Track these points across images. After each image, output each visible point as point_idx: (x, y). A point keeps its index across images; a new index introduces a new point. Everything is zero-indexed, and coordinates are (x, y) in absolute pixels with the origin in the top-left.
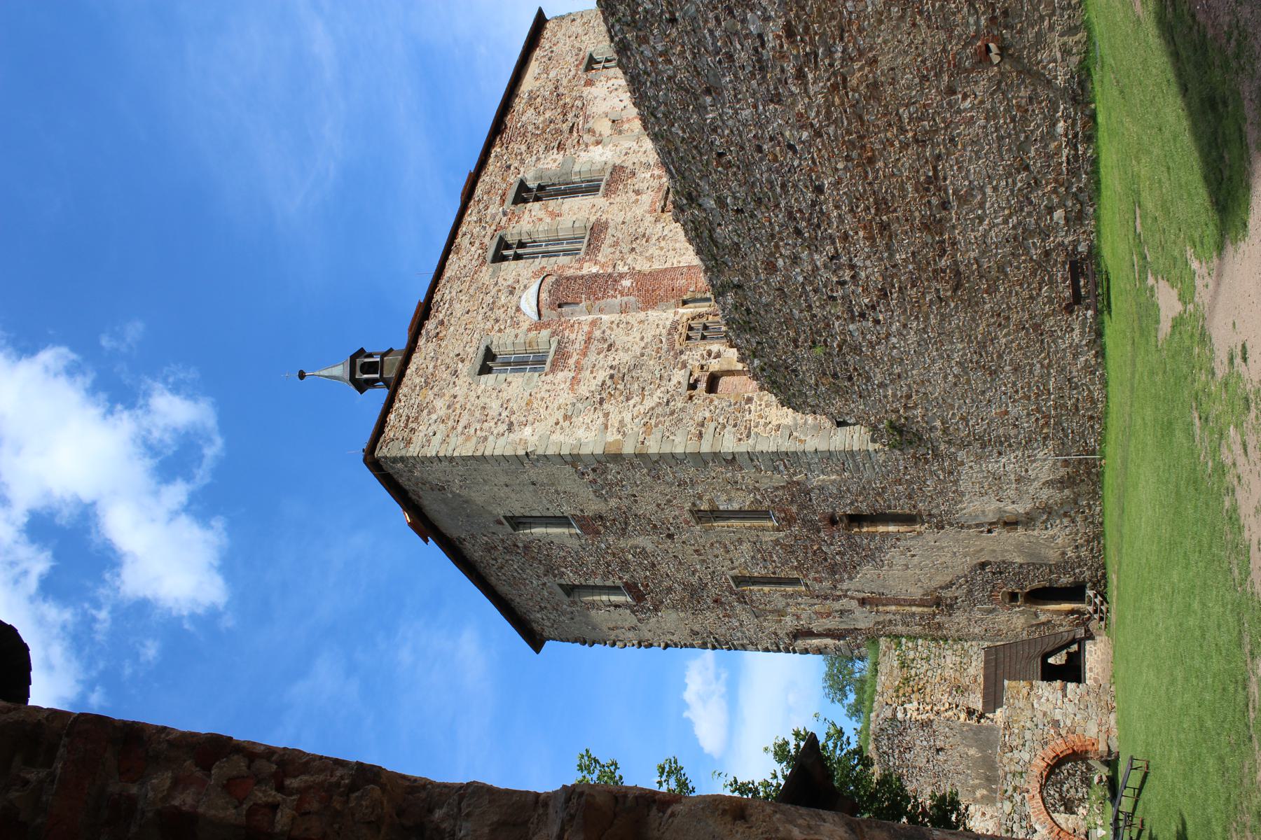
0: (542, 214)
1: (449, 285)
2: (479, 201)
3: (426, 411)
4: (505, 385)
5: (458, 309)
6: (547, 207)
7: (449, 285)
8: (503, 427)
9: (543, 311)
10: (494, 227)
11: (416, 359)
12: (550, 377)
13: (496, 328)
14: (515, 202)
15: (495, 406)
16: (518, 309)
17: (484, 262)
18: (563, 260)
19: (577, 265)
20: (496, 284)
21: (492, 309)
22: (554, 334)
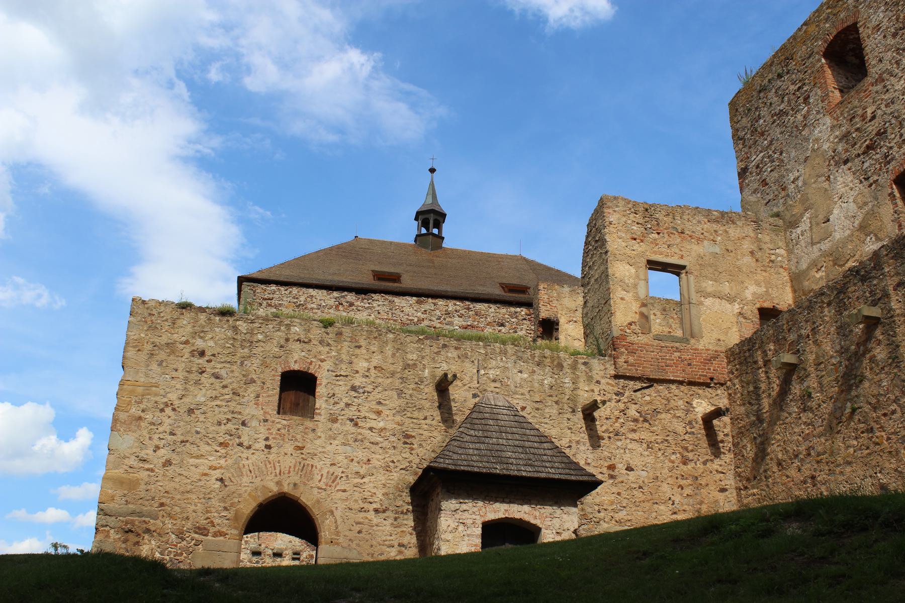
1: (386, 303)
2: (468, 309)
7: (386, 303)
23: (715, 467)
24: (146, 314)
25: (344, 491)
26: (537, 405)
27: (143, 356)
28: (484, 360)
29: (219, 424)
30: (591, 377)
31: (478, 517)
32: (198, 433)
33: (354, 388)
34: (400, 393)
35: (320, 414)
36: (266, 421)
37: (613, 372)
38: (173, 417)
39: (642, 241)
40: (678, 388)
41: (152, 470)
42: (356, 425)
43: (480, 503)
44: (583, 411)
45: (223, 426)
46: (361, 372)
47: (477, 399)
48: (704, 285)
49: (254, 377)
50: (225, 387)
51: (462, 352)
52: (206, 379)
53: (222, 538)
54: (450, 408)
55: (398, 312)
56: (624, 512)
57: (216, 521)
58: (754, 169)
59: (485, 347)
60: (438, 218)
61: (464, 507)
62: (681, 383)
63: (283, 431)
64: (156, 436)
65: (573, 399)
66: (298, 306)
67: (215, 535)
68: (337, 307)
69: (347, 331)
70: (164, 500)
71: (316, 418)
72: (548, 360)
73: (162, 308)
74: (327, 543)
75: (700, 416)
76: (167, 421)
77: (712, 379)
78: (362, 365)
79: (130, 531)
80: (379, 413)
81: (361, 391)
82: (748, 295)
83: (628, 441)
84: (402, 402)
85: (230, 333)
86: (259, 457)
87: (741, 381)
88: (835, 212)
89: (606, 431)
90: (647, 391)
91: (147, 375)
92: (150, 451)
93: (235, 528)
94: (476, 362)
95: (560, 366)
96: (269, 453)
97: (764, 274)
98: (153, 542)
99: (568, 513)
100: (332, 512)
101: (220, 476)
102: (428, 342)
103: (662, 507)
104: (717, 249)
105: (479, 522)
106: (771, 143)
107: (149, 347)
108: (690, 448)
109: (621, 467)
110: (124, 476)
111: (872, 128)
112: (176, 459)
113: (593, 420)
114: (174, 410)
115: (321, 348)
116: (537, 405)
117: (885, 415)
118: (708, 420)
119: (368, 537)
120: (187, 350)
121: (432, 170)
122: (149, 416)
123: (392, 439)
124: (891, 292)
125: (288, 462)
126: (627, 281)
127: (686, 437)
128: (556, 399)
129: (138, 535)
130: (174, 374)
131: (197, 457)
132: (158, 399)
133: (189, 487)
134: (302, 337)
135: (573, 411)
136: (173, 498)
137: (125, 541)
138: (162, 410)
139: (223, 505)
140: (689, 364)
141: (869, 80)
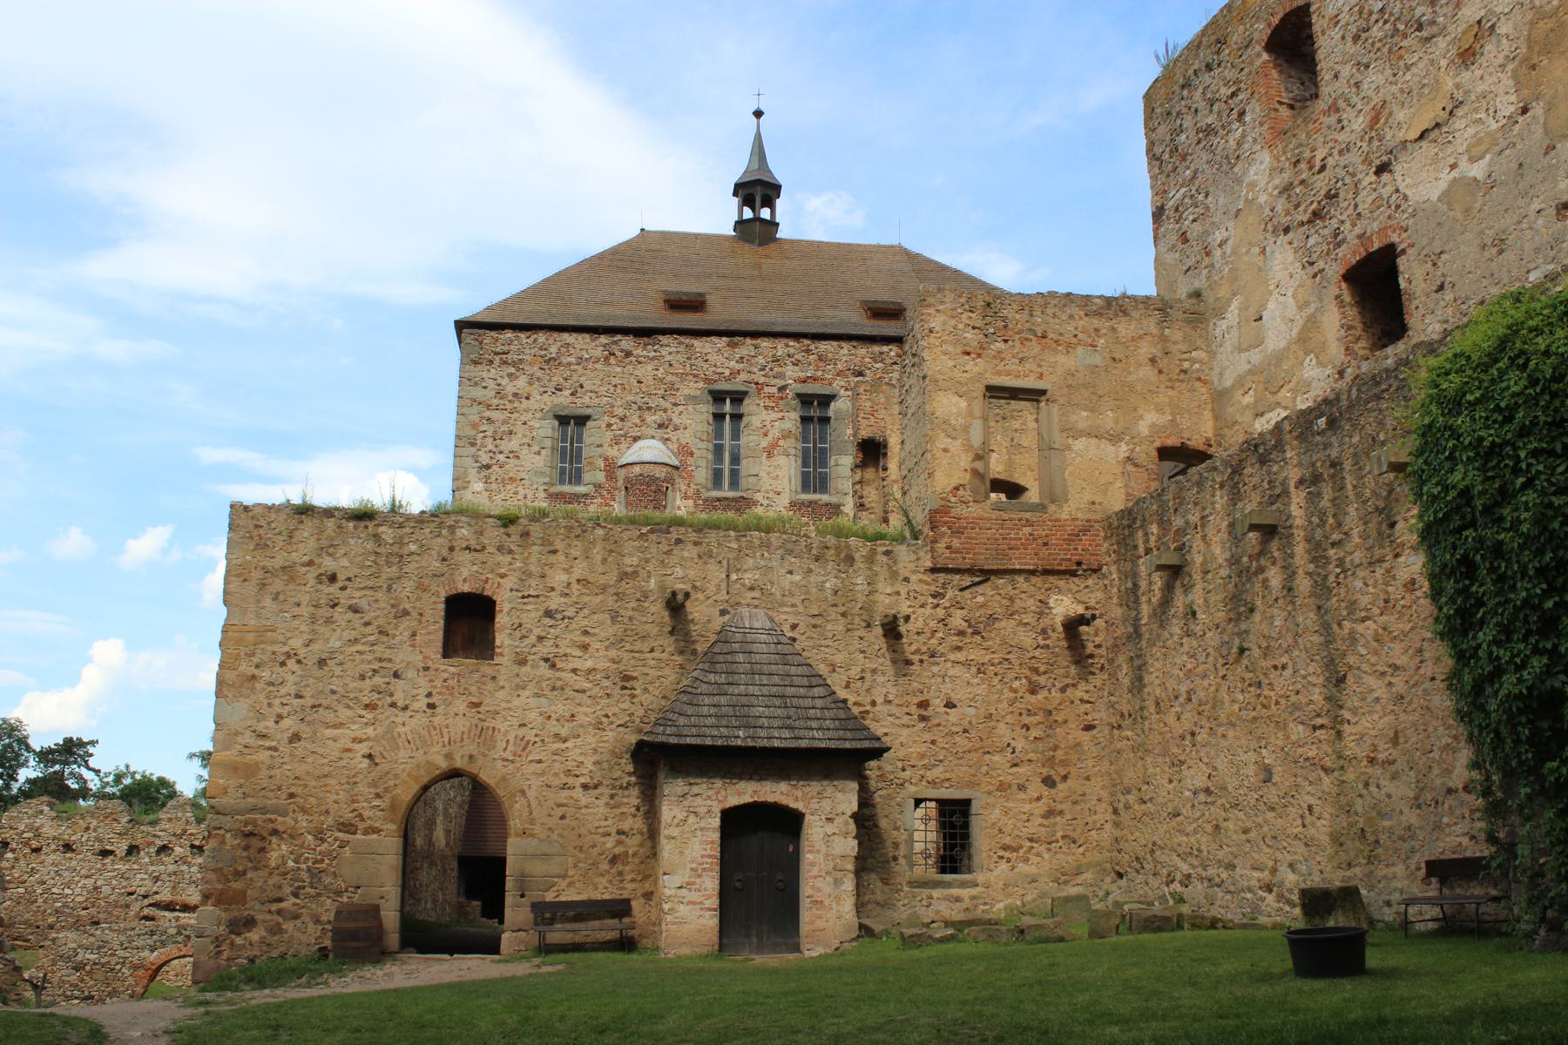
0: (774, 433)
2: (808, 351)
3: (513, 370)
4: (536, 448)
5: (646, 371)
6: (784, 437)
8: (485, 459)
9: (624, 471)
10: (762, 380)
11: (579, 341)
12: (543, 495)
13: (613, 420)
14: (799, 395)
15: (513, 444)
16: (636, 439)
17: (707, 380)
18: (702, 475)
19: (691, 492)
20: (675, 405)
21: (640, 408)
22: (598, 486)
23: (1079, 694)
24: (251, 527)
25: (540, 762)
26: (814, 621)
27: (251, 589)
28: (737, 559)
29: (362, 677)
30: (896, 573)
31: (715, 803)
32: (333, 692)
33: (549, 614)
34: (615, 617)
35: (501, 654)
36: (427, 669)
37: (929, 564)
38: (299, 672)
39: (979, 356)
40: (1027, 580)
41: (275, 749)
42: (553, 666)
43: (718, 783)
44: (883, 625)
45: (368, 681)
46: (559, 589)
47: (727, 617)
48: (1074, 418)
49: (408, 606)
50: (367, 624)
51: (704, 548)
52: (341, 616)
53: (375, 836)
54: (687, 634)
55: (699, 362)
56: (941, 769)
57: (366, 814)
58: (1172, 214)
59: (737, 539)
60: (769, 192)
61: (696, 789)
62: (1033, 572)
63: (451, 682)
64: (277, 702)
65: (868, 608)
66: (548, 362)
67: (366, 832)
68: (606, 359)
69: (536, 529)
70: (293, 790)
71: (497, 660)
72: (832, 552)
73: (273, 516)
74: (517, 835)
75: (1059, 620)
76: (291, 679)
77: (1079, 564)
78: (559, 578)
79: (251, 834)
80: (585, 647)
81: (559, 616)
82: (1143, 428)
83: (949, 665)
84: (618, 629)
85: (370, 546)
86: (420, 720)
87: (1119, 570)
88: (1271, 305)
89: (917, 651)
90: (980, 589)
91: (258, 616)
92: (271, 724)
93: (392, 821)
94: (725, 563)
95: (850, 560)
96: (433, 715)
97: (1170, 392)
98: (284, 847)
99: (842, 791)
100: (523, 792)
101: (367, 751)
102: (653, 537)
103: (997, 758)
104: (1097, 360)
105: (717, 811)
106: (1194, 177)
107: (257, 575)
108: (1042, 669)
109: (937, 703)
110: (239, 759)
111: (1321, 183)
112: (306, 731)
113: (899, 636)
114: (299, 662)
115: (500, 558)
116: (814, 621)
117: (1275, 667)
118: (1073, 626)
119: (574, 823)
120: (312, 574)
121: (758, 114)
122: (265, 674)
123: (606, 683)
124: (1292, 489)
125: (461, 725)
126: (953, 422)
127: (1037, 653)
128: (843, 609)
129: (264, 838)
130: (296, 611)
131: (335, 727)
132: (275, 648)
133: (327, 769)
134: (473, 543)
135: (869, 626)
136: (306, 786)
137: (247, 848)
138: (283, 664)
139: (373, 790)
140: (1045, 544)
141: (1321, 105)
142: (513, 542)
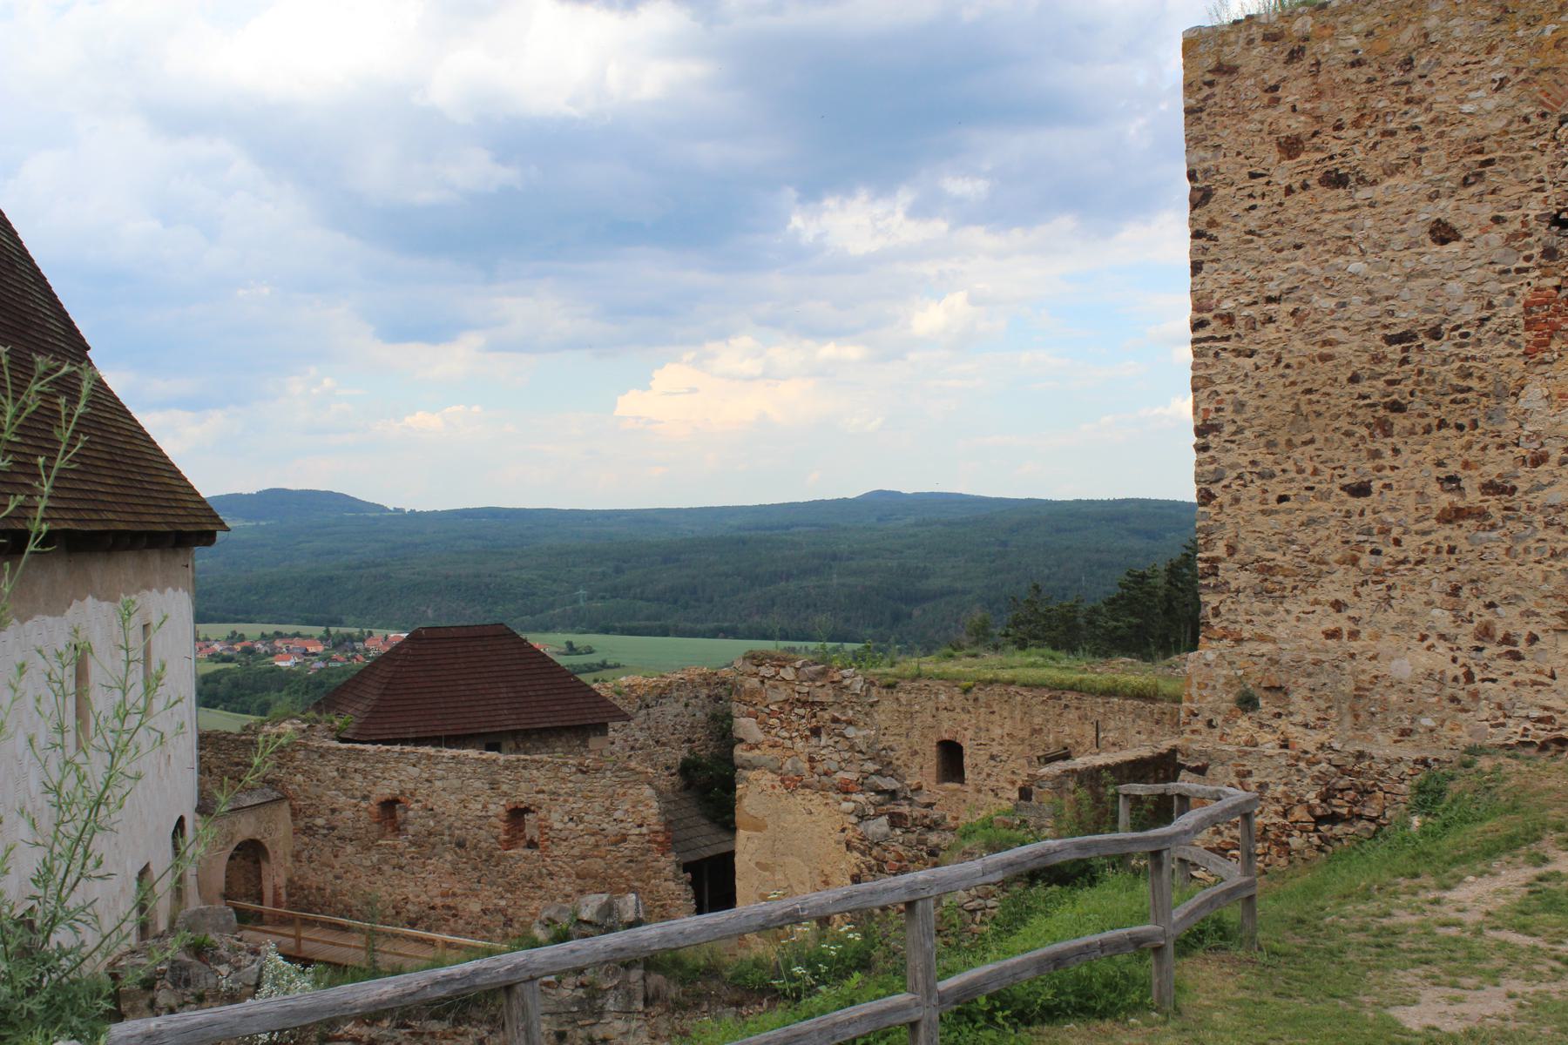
33: (992, 757)
51: (1081, 712)
78: (997, 732)
85: (895, 706)
142: (970, 705)
